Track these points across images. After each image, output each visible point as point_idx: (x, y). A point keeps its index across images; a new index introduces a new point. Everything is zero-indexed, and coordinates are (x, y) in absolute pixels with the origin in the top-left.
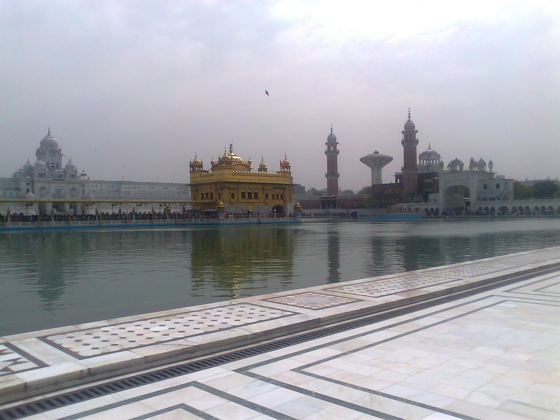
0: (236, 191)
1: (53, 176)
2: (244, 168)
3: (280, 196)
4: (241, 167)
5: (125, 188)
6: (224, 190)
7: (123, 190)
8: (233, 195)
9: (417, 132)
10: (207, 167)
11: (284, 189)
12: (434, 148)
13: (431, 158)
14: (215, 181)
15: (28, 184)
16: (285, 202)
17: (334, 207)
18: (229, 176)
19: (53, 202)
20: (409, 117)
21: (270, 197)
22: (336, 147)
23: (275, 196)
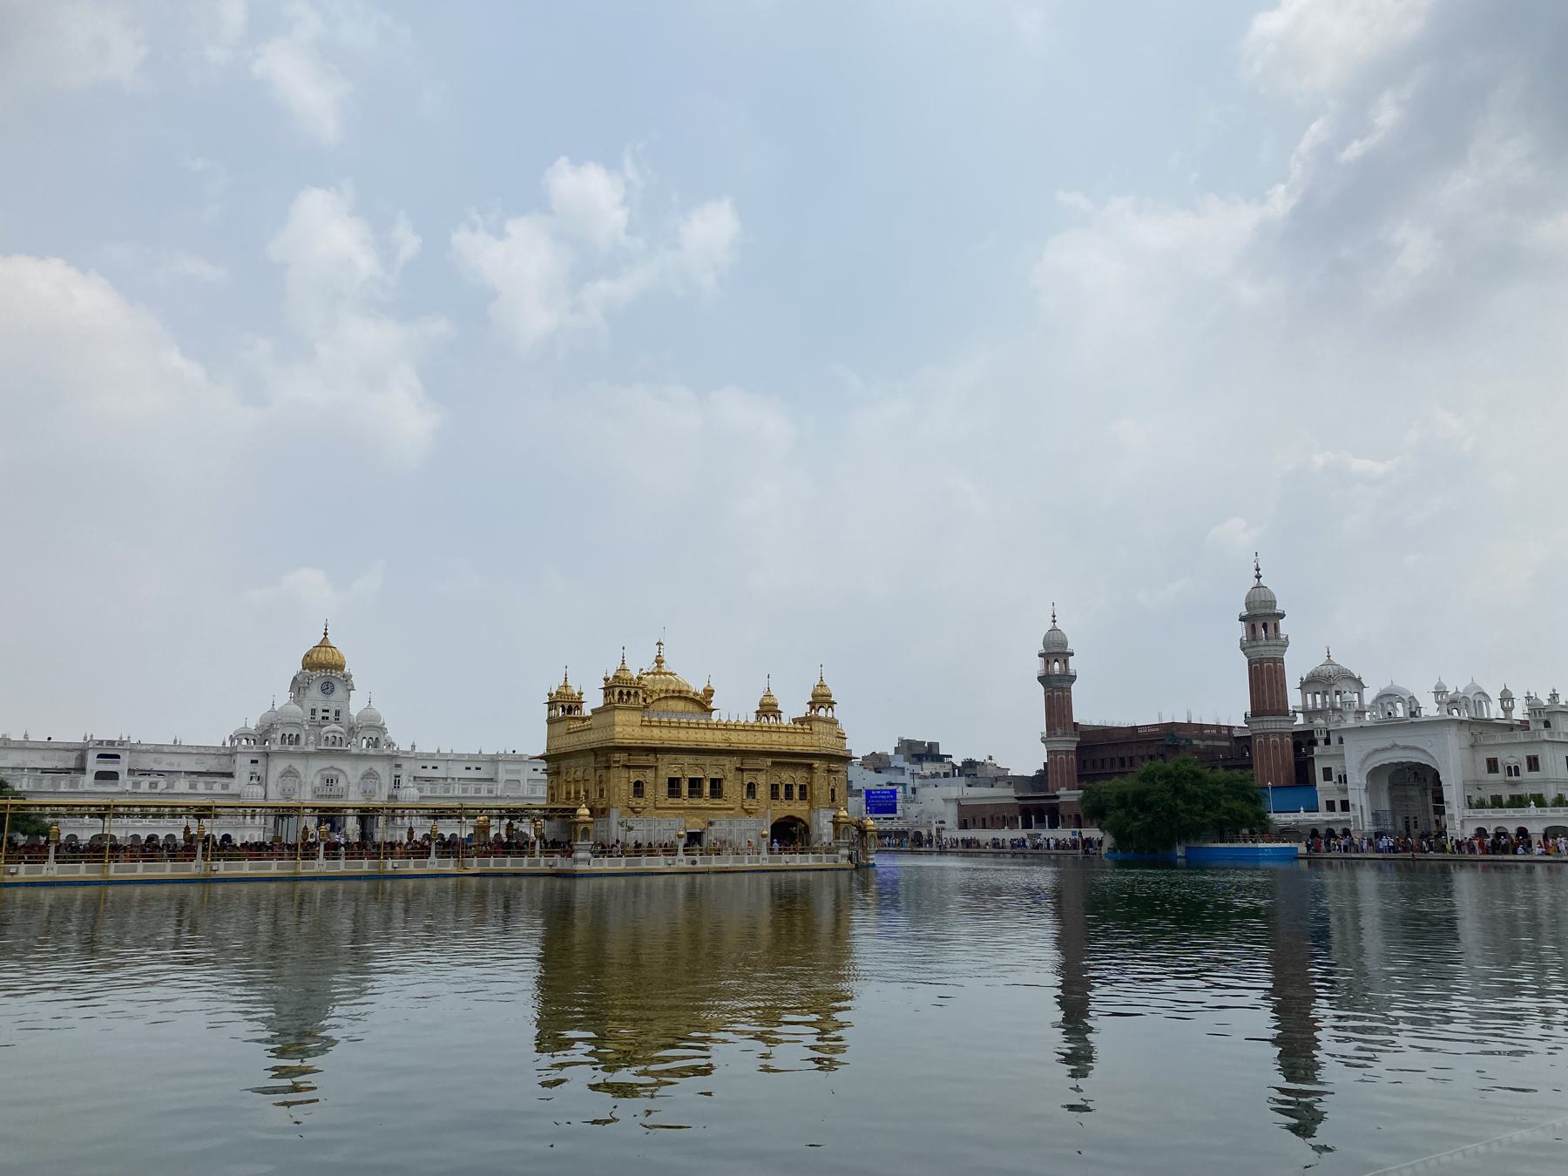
0: (650, 774)
1: (318, 738)
2: (691, 707)
3: (796, 790)
4: (680, 705)
5: (507, 771)
6: (613, 772)
7: (502, 776)
8: (638, 788)
9: (1282, 616)
12: (1345, 661)
13: (1334, 688)
17: (1053, 825)
18: (629, 730)
19: (314, 808)
20: (1258, 577)
21: (763, 791)
22: (1066, 662)
23: (782, 790)
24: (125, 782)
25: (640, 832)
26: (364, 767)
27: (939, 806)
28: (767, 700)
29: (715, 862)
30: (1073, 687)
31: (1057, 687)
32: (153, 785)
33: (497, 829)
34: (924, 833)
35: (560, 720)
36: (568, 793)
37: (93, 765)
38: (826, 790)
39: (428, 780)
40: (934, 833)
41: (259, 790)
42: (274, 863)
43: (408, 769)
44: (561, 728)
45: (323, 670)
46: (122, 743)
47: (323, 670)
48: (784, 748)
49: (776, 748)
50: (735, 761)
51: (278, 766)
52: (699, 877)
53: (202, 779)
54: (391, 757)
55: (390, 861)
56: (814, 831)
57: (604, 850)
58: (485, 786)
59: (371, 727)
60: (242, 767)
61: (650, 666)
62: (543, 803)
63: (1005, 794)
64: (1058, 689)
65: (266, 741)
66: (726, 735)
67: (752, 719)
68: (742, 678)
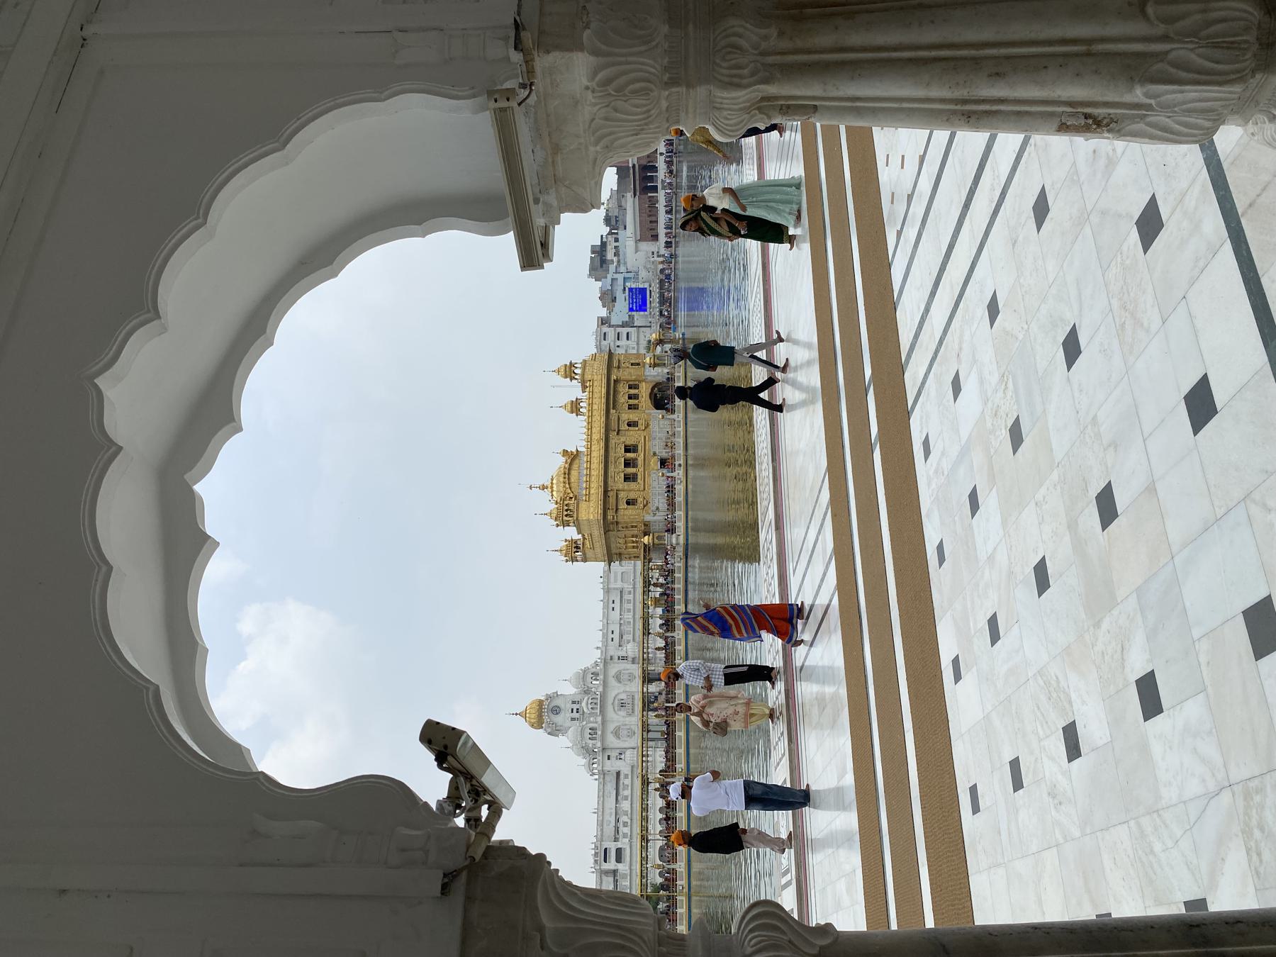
0: (622, 495)
2: (575, 466)
3: (633, 391)
4: (574, 473)
7: (619, 585)
10: (571, 533)
17: (654, 169)
21: (633, 416)
23: (632, 402)
24: (623, 843)
25: (660, 501)
26: (612, 682)
27: (641, 254)
28: (569, 407)
29: (679, 451)
32: (625, 824)
34: (661, 266)
35: (584, 554)
37: (612, 864)
38: (633, 370)
39: (621, 636)
40: (661, 259)
41: (628, 753)
42: (677, 733)
43: (614, 651)
44: (589, 553)
45: (543, 715)
46: (596, 847)
47: (543, 715)
48: (604, 400)
49: (604, 407)
50: (613, 435)
51: (612, 741)
52: (690, 462)
53: (621, 792)
56: (660, 379)
58: (626, 597)
59: (584, 678)
61: (548, 491)
62: (639, 564)
65: (594, 750)
66: (595, 442)
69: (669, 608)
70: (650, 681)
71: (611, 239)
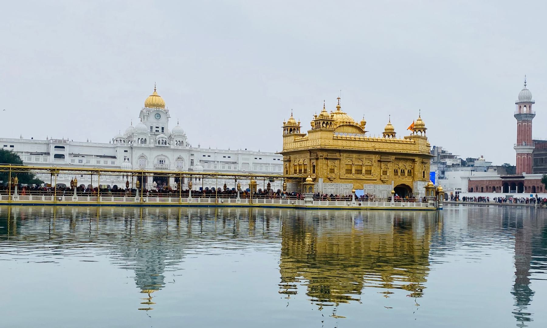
0: (337, 162)
2: (354, 130)
3: (406, 172)
4: (350, 129)
11: (413, 161)
14: (310, 148)
15: (125, 151)
16: (413, 179)
17: (520, 191)
18: (327, 141)
19: (155, 173)
22: (530, 107)
23: (399, 171)
24: (68, 159)
26: (177, 155)
30: (534, 120)
31: (524, 120)
33: (262, 186)
36: (295, 171)
39: (206, 162)
42: (170, 199)
45: (155, 109)
46: (65, 142)
47: (155, 109)
49: (398, 151)
50: (377, 157)
51: (137, 154)
54: (189, 151)
55: (220, 199)
56: (414, 191)
57: (317, 197)
60: (120, 154)
63: (494, 176)
64: (524, 121)
66: (373, 144)
67: (381, 137)
68: (381, 117)
69: (245, 195)
70: (177, 180)
71: (459, 162)
